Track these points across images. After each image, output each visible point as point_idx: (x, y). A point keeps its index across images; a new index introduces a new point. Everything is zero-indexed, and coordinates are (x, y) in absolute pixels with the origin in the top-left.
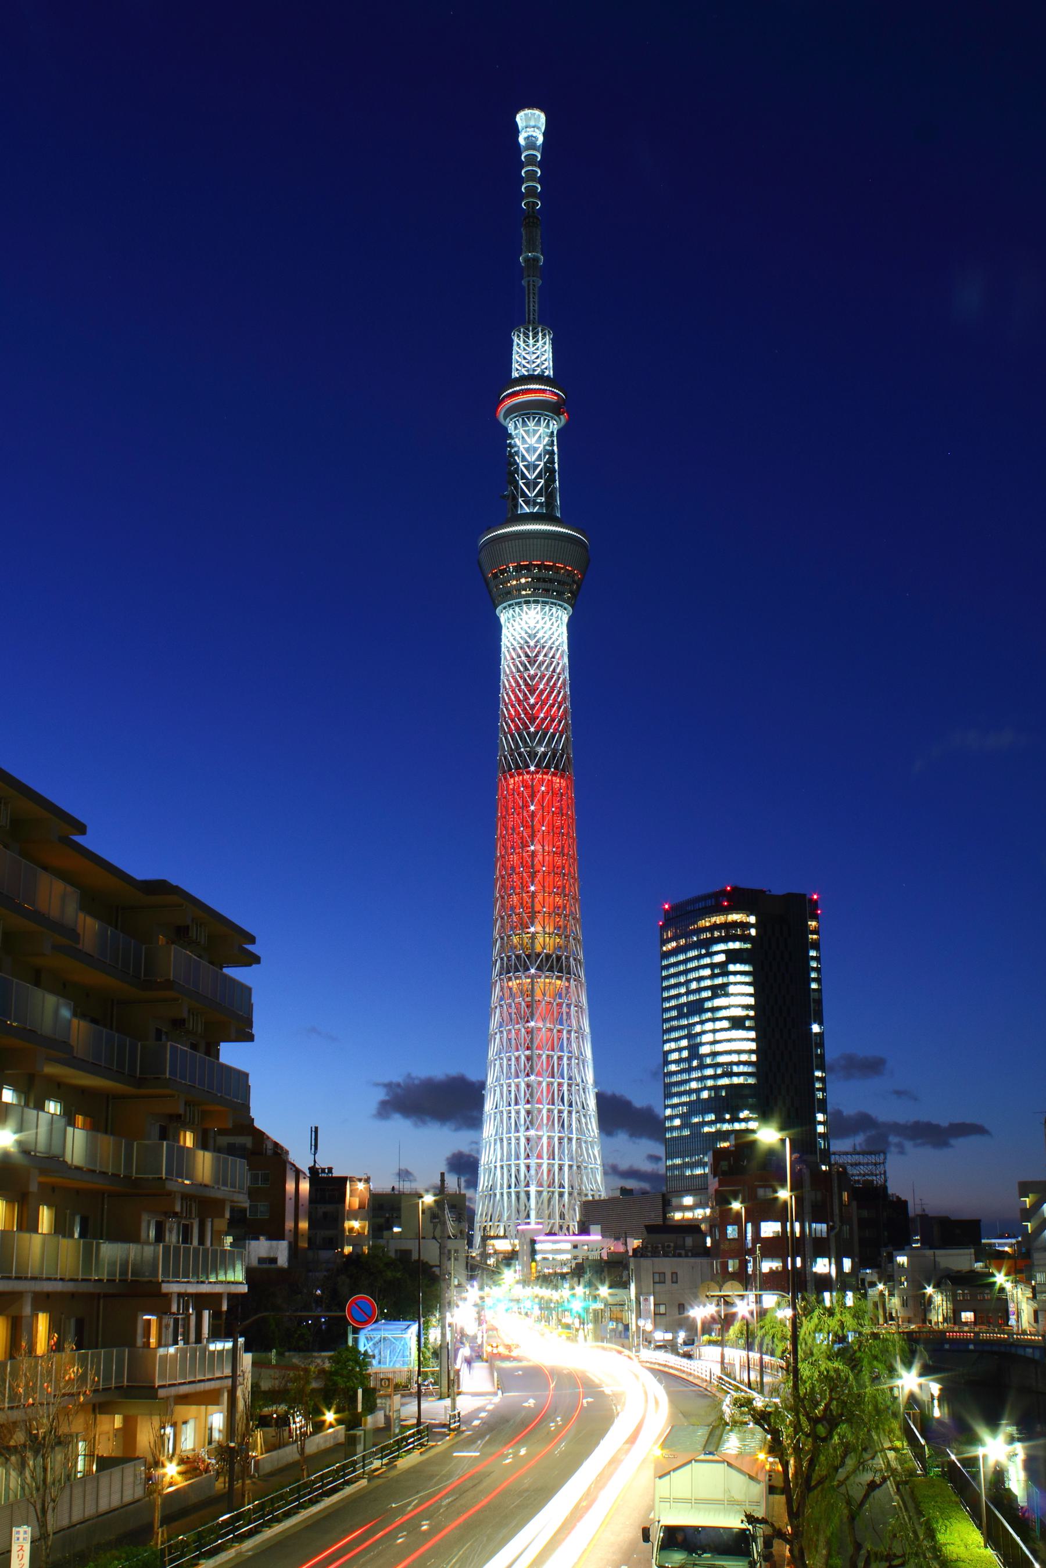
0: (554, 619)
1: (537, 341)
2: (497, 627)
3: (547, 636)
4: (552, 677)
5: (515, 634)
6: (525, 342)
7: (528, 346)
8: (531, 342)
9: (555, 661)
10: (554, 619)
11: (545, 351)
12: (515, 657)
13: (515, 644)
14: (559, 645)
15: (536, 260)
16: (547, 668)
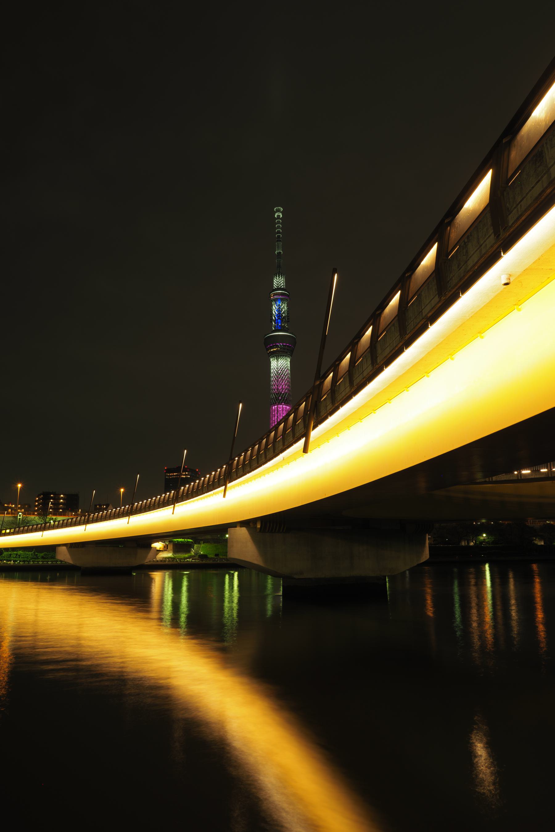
0: (284, 360)
1: (280, 278)
2: (270, 363)
3: (282, 365)
4: (283, 377)
5: (273, 365)
6: (276, 278)
7: (277, 279)
8: (278, 278)
9: (284, 372)
10: (284, 360)
11: (282, 280)
12: (273, 371)
13: (273, 368)
14: (286, 367)
15: (280, 253)
16: (282, 375)
